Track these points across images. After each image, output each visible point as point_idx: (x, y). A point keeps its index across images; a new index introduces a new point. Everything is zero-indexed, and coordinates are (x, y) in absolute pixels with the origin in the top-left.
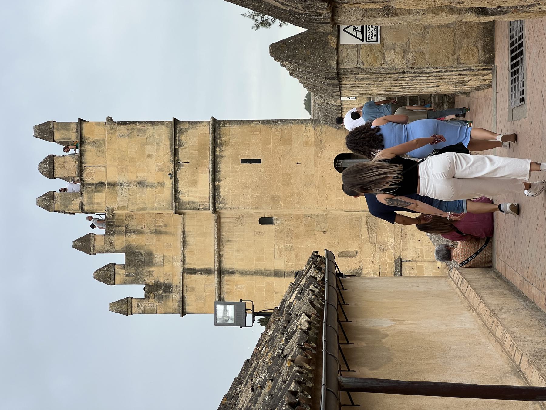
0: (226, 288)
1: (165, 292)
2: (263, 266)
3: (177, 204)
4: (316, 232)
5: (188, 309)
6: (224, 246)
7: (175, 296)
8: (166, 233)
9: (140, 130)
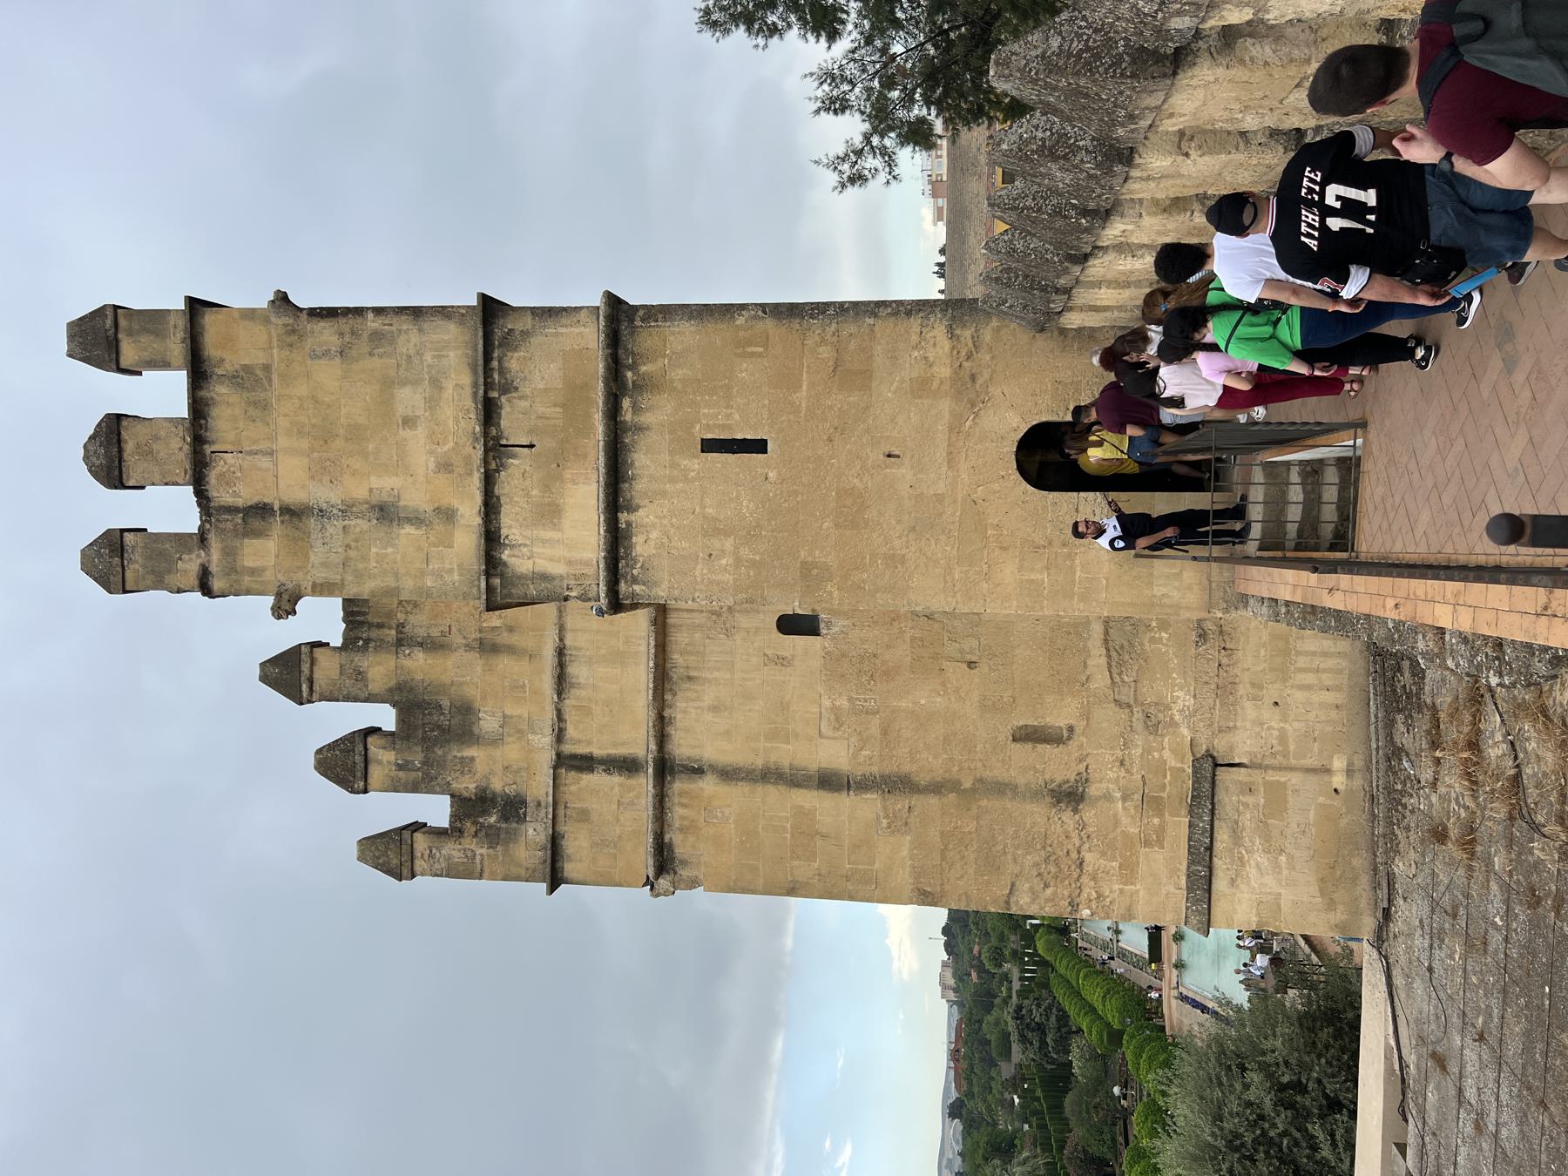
0: (677, 813)
1: (505, 818)
2: (786, 755)
3: (497, 581)
4: (946, 664)
5: (569, 869)
6: (674, 695)
7: (534, 832)
8: (511, 650)
9: (376, 337)
